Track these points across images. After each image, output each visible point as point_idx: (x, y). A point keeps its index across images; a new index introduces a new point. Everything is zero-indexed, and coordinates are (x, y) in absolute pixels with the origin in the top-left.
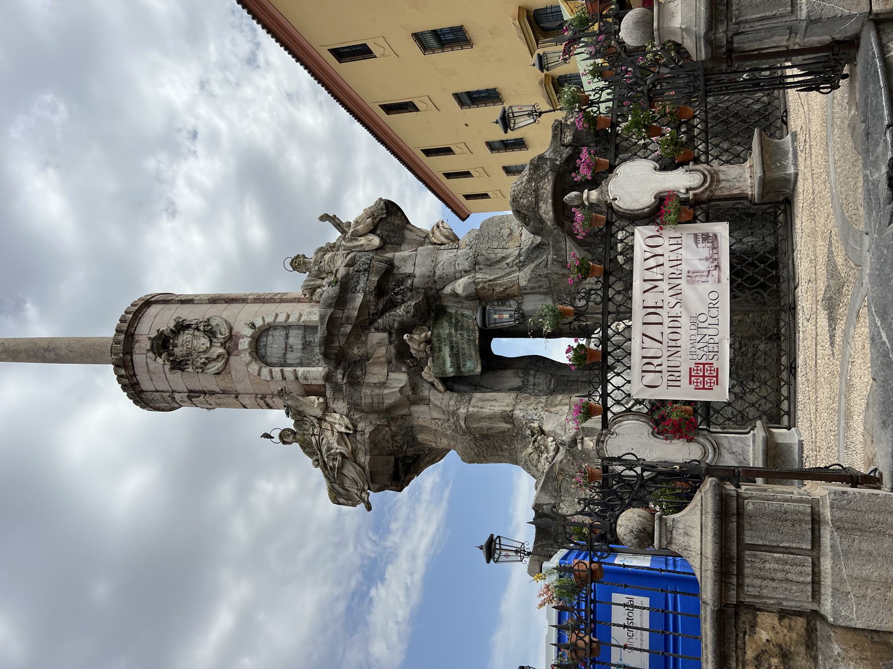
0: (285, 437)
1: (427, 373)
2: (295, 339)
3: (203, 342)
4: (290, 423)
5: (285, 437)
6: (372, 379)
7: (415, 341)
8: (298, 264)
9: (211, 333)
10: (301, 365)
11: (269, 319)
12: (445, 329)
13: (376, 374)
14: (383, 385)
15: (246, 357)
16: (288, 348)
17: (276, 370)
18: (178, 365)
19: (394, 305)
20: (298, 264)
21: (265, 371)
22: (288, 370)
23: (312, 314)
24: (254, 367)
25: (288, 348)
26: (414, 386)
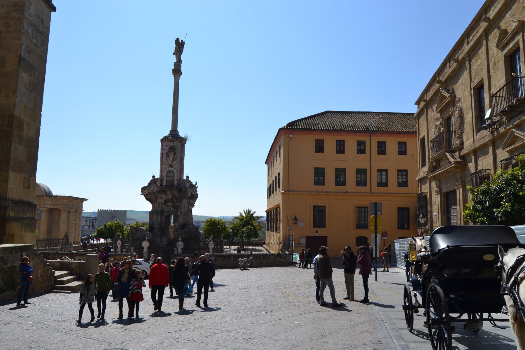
0: (154, 177)
1: (164, 206)
2: (171, 179)
3: (171, 159)
4: (156, 177)
5: (154, 177)
6: (163, 196)
7: (169, 204)
8: (187, 177)
9: (173, 161)
10: (167, 180)
11: (176, 174)
12: (172, 209)
13: (164, 196)
14: (162, 198)
15: (168, 169)
16: (170, 178)
17: (165, 175)
18: (167, 154)
19: (177, 199)
20: (187, 177)
21: (165, 173)
22: (165, 178)
23: (176, 183)
24: (166, 171)
25: (170, 178)
26: (162, 203)
